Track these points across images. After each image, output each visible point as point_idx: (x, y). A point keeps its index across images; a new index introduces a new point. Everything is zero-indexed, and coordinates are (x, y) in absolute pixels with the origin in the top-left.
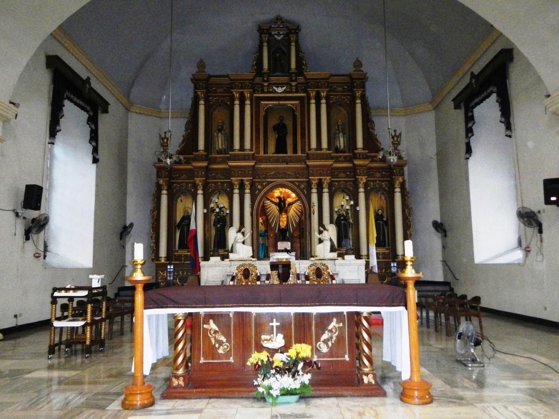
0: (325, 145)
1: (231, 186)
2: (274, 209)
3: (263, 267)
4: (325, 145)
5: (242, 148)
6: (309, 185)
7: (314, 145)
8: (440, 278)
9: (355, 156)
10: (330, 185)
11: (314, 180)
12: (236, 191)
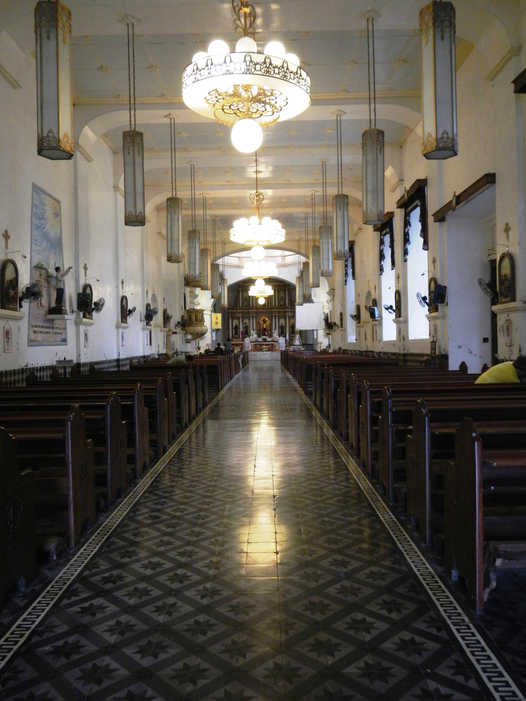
0: (277, 304)
1: (250, 316)
2: (262, 322)
3: (260, 339)
4: (277, 304)
5: (253, 306)
6: (272, 317)
7: (274, 305)
8: (311, 343)
9: (285, 308)
10: (279, 316)
11: (274, 315)
12: (251, 318)
